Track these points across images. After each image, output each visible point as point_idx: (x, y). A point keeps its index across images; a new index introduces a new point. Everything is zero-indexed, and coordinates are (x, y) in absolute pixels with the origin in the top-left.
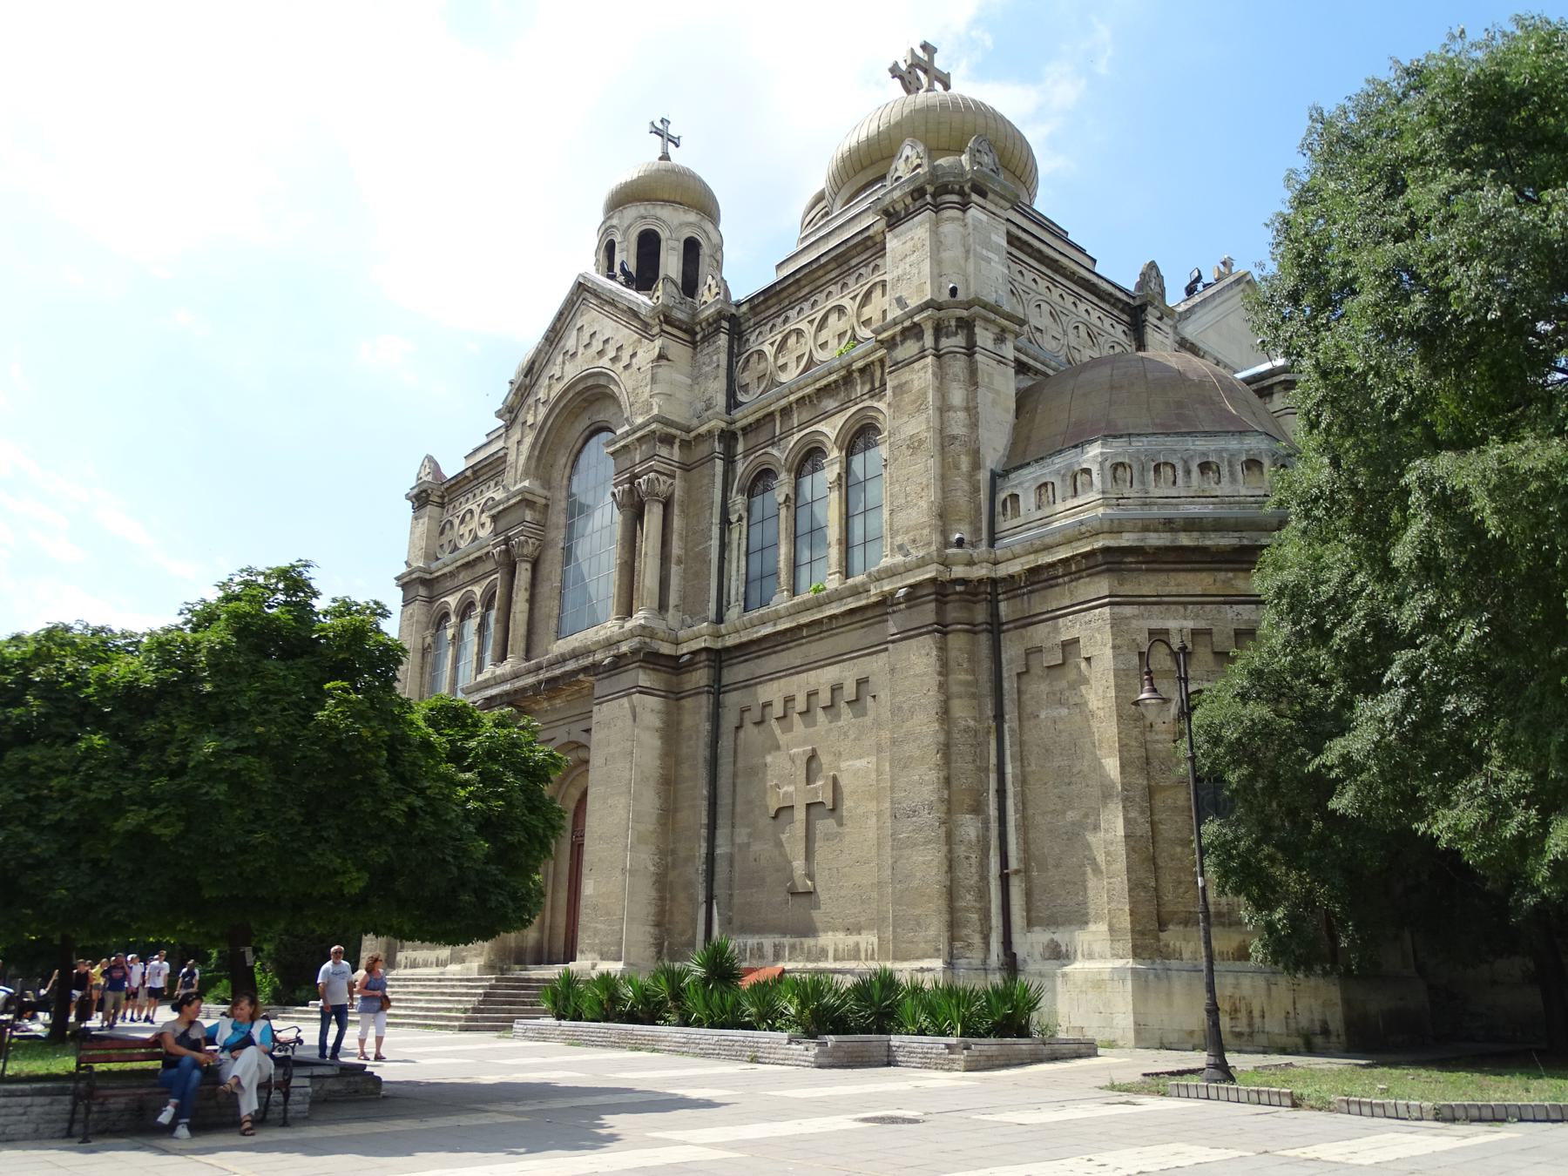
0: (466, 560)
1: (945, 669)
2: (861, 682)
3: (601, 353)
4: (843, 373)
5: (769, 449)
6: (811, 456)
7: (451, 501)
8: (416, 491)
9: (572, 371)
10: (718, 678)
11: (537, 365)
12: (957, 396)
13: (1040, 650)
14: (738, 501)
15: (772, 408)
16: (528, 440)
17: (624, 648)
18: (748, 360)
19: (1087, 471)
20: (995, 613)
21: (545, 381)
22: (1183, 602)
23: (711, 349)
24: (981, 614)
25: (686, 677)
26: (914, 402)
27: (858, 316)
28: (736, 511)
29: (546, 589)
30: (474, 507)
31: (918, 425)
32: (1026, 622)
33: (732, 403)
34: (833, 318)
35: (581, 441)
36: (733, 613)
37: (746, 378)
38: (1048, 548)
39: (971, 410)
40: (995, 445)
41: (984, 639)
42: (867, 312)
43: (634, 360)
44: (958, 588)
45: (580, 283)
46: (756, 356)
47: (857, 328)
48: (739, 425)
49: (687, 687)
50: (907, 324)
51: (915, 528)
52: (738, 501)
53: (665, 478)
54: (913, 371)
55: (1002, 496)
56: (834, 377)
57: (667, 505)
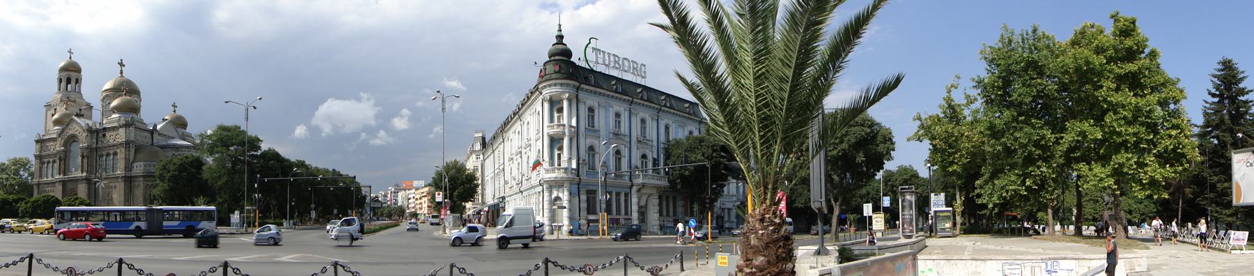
1: (125, 186)
6: (108, 155)
9: (71, 132)
12: (128, 153)
14: (98, 158)
22: (150, 181)
24: (129, 180)
29: (67, 164)
31: (123, 156)
32: (134, 181)
33: (97, 144)
39: (129, 154)
40: (132, 158)
52: (98, 158)
57: (88, 157)
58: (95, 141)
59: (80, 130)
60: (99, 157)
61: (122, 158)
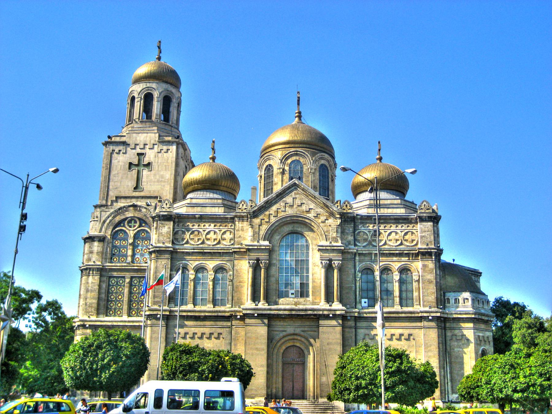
0: (202, 251)
2: (410, 335)
3: (308, 212)
4: (401, 252)
5: (370, 263)
7: (179, 222)
8: (166, 213)
9: (290, 212)
10: (356, 324)
11: (270, 201)
13: (456, 335)
15: (374, 252)
16: (264, 228)
17: (338, 313)
18: (359, 232)
19: (467, 299)
20: (445, 325)
21: (274, 208)
23: (349, 226)
25: (346, 322)
26: (429, 270)
27: (403, 238)
28: (358, 277)
30: (201, 230)
34: (393, 234)
35: (286, 233)
36: (359, 306)
37: (359, 238)
38: (460, 314)
41: (443, 331)
42: (406, 237)
43: (327, 221)
44: (442, 319)
45: (295, 183)
46: (362, 233)
47: (403, 241)
48: (359, 252)
49: (347, 325)
50: (429, 250)
51: (431, 302)
53: (337, 262)
54: (429, 262)
55: (446, 298)
56: (397, 252)
58: (351, 238)
59: (320, 210)
60: (361, 272)
61: (430, 282)
